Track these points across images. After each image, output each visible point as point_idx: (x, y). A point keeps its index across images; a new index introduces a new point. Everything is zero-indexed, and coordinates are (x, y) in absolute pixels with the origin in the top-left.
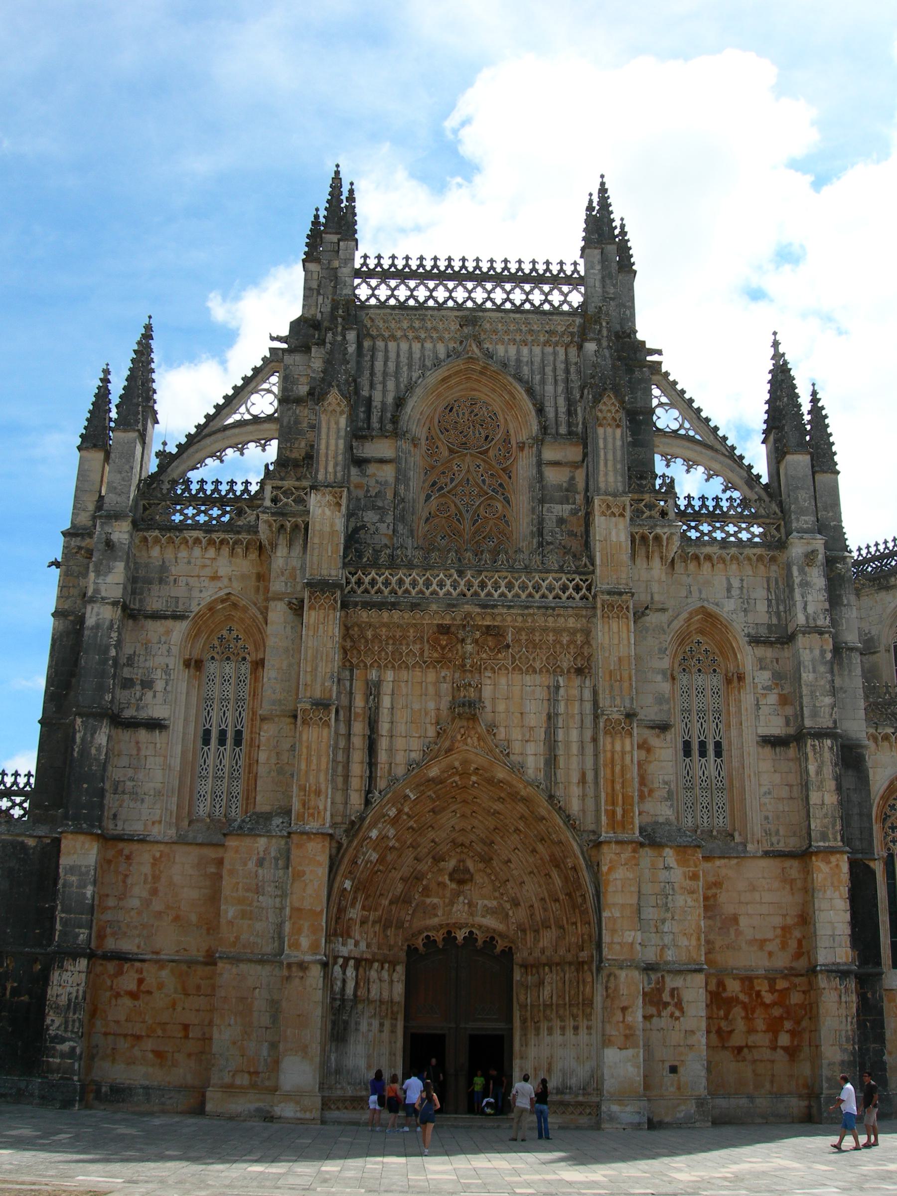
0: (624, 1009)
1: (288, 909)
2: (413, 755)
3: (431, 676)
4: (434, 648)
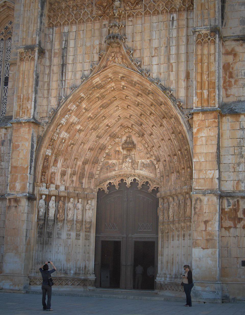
0: (206, 222)
1: (10, 167)
2: (86, 73)
3: (97, 25)
4: (99, 9)
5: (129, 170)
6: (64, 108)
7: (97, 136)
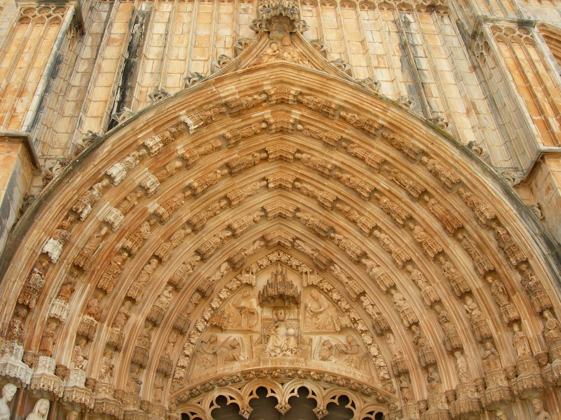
5: (289, 358)
6: (124, 136)
7: (197, 252)
